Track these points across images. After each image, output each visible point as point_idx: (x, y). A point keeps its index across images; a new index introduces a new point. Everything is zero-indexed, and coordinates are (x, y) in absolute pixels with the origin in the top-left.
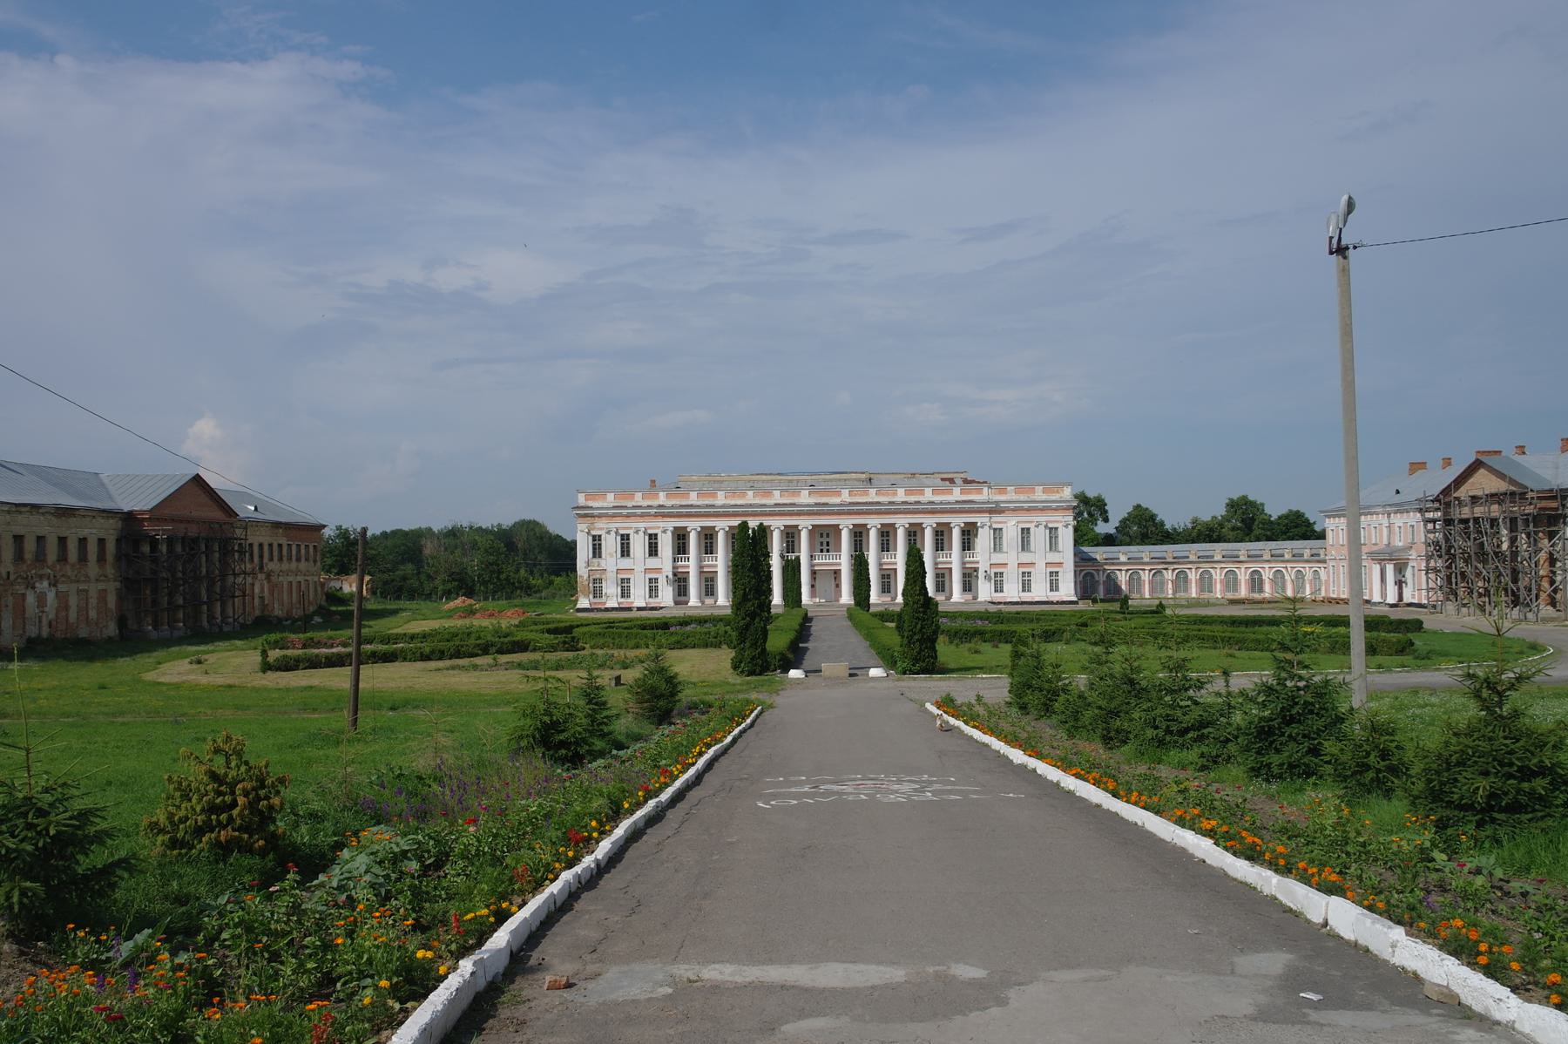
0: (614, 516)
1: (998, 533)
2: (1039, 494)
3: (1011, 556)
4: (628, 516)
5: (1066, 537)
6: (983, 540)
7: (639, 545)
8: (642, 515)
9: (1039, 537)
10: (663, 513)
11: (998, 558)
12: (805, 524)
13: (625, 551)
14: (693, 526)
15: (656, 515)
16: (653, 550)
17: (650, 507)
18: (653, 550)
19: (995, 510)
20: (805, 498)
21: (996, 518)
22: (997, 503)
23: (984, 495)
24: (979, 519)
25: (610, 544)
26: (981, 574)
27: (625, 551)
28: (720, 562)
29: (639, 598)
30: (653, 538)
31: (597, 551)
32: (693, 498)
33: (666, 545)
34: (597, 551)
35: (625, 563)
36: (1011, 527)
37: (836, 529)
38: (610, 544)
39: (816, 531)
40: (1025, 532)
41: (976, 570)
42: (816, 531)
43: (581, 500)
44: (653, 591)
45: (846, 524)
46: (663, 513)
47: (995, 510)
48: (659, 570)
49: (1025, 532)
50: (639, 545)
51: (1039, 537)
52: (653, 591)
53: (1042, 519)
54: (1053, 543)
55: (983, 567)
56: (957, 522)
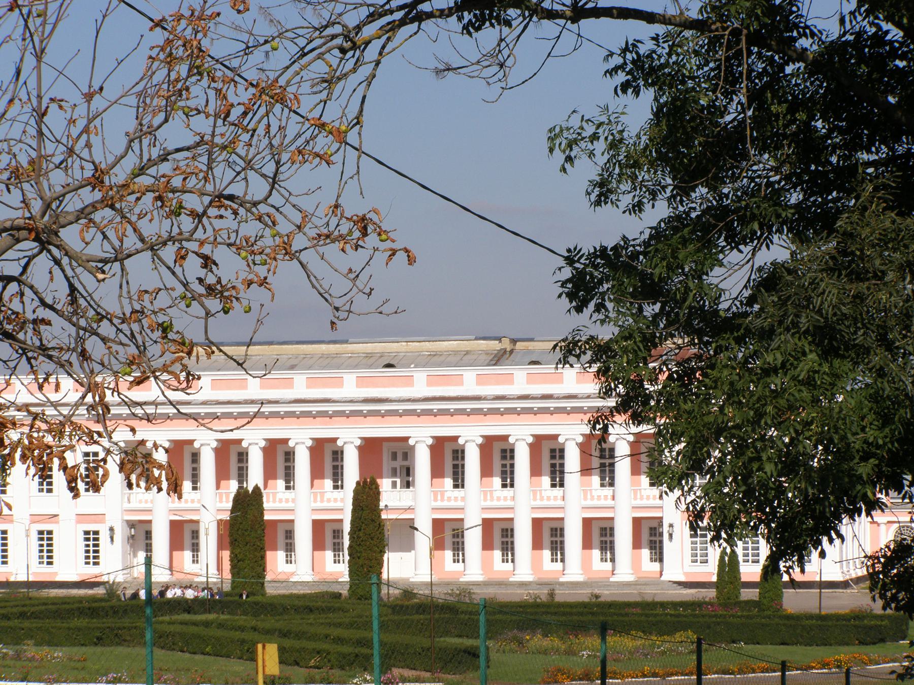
12: (349, 436)
29: (69, 567)
39: (370, 448)
42: (370, 448)
44: (92, 554)
45: (421, 436)
48: (99, 517)
52: (92, 554)
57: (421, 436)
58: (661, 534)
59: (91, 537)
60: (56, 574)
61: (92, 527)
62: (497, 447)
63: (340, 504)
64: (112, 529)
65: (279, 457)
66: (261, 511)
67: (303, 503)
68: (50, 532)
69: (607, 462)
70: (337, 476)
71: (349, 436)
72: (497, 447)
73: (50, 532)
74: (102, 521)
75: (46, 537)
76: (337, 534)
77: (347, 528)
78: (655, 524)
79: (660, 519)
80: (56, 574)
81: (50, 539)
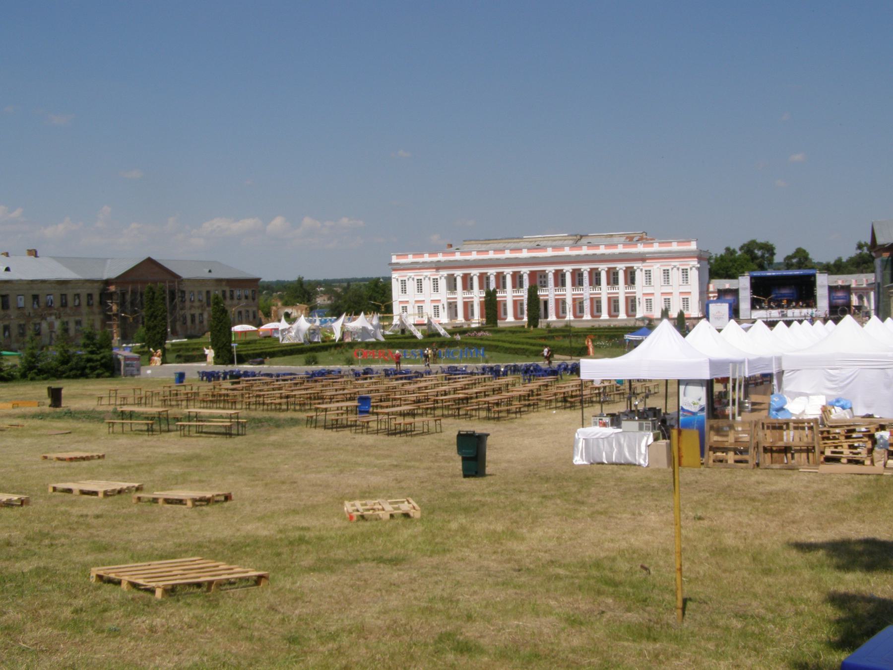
1: (648, 273)
2: (675, 247)
3: (657, 288)
5: (694, 275)
6: (639, 277)
7: (427, 285)
9: (676, 276)
10: (438, 266)
11: (649, 290)
12: (525, 271)
13: (420, 289)
14: (459, 273)
16: (436, 288)
18: (436, 288)
20: (525, 254)
24: (636, 265)
25: (411, 286)
27: (420, 289)
30: (435, 281)
31: (404, 291)
32: (458, 257)
33: (443, 284)
34: (404, 291)
36: (656, 268)
38: (411, 286)
39: (532, 275)
40: (666, 272)
41: (635, 297)
43: (394, 260)
44: (437, 314)
45: (550, 270)
46: (438, 266)
49: (666, 272)
50: (427, 285)
55: (638, 295)
57: (550, 270)
59: (436, 308)
62: (577, 273)
63: (524, 294)
65: (538, 280)
66: (496, 297)
67: (508, 296)
70: (521, 286)
71: (525, 271)
72: (577, 273)
76: (522, 304)
77: (525, 302)
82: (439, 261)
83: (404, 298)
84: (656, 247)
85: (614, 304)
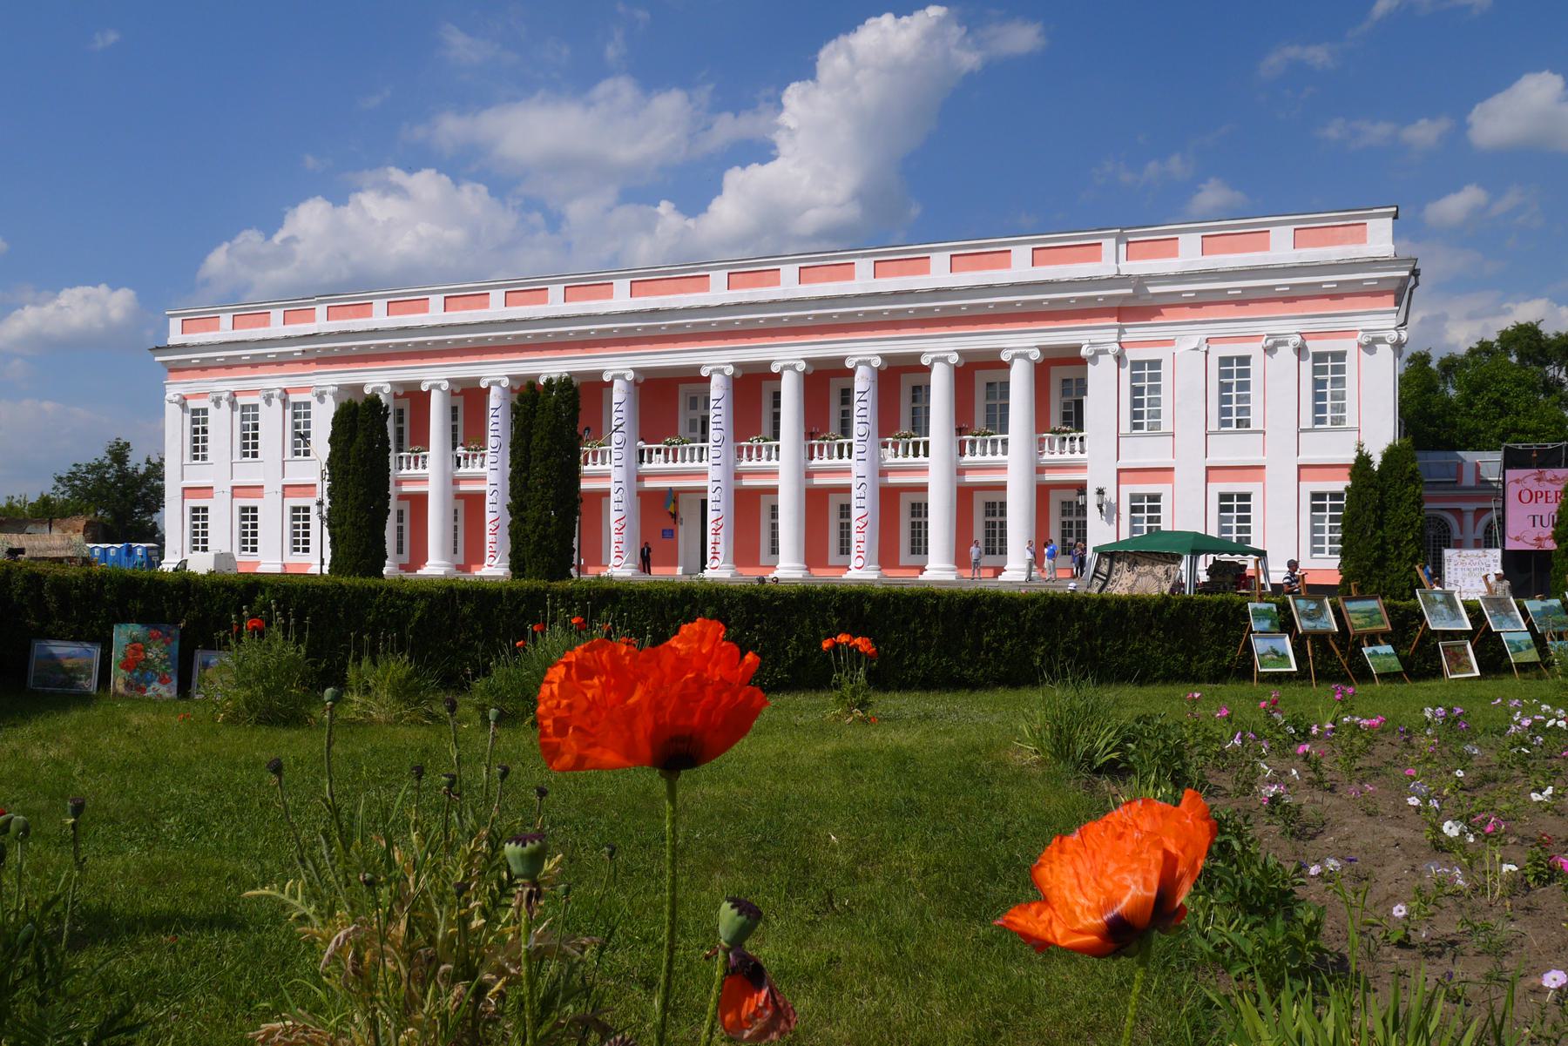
0: (229, 365)
4: (255, 363)
6: (1104, 392)
8: (280, 362)
9: (1279, 386)
15: (308, 359)
17: (288, 340)
19: (1135, 306)
21: (1136, 332)
22: (1141, 281)
23: (1110, 260)
25: (222, 428)
26: (1092, 500)
27: (250, 445)
28: (490, 473)
31: (198, 448)
34: (198, 448)
35: (249, 473)
37: (695, 379)
38: (222, 428)
40: (1235, 372)
41: (1081, 488)
45: (718, 362)
47: (1135, 306)
49: (1235, 372)
51: (1279, 386)
53: (1288, 325)
54: (1325, 402)
56: (1019, 346)
57: (718, 362)
58: (1082, 510)
59: (300, 514)
60: (258, 563)
61: (301, 502)
64: (320, 503)
68: (255, 509)
69: (998, 402)
73: (255, 509)
74: (312, 494)
75: (249, 516)
78: (1070, 495)
79: (1081, 488)
80: (258, 563)
81: (254, 518)
82: (313, 337)
83: (198, 475)
84: (1189, 252)
85: (979, 511)
